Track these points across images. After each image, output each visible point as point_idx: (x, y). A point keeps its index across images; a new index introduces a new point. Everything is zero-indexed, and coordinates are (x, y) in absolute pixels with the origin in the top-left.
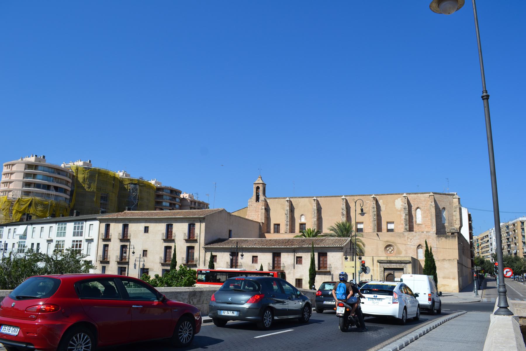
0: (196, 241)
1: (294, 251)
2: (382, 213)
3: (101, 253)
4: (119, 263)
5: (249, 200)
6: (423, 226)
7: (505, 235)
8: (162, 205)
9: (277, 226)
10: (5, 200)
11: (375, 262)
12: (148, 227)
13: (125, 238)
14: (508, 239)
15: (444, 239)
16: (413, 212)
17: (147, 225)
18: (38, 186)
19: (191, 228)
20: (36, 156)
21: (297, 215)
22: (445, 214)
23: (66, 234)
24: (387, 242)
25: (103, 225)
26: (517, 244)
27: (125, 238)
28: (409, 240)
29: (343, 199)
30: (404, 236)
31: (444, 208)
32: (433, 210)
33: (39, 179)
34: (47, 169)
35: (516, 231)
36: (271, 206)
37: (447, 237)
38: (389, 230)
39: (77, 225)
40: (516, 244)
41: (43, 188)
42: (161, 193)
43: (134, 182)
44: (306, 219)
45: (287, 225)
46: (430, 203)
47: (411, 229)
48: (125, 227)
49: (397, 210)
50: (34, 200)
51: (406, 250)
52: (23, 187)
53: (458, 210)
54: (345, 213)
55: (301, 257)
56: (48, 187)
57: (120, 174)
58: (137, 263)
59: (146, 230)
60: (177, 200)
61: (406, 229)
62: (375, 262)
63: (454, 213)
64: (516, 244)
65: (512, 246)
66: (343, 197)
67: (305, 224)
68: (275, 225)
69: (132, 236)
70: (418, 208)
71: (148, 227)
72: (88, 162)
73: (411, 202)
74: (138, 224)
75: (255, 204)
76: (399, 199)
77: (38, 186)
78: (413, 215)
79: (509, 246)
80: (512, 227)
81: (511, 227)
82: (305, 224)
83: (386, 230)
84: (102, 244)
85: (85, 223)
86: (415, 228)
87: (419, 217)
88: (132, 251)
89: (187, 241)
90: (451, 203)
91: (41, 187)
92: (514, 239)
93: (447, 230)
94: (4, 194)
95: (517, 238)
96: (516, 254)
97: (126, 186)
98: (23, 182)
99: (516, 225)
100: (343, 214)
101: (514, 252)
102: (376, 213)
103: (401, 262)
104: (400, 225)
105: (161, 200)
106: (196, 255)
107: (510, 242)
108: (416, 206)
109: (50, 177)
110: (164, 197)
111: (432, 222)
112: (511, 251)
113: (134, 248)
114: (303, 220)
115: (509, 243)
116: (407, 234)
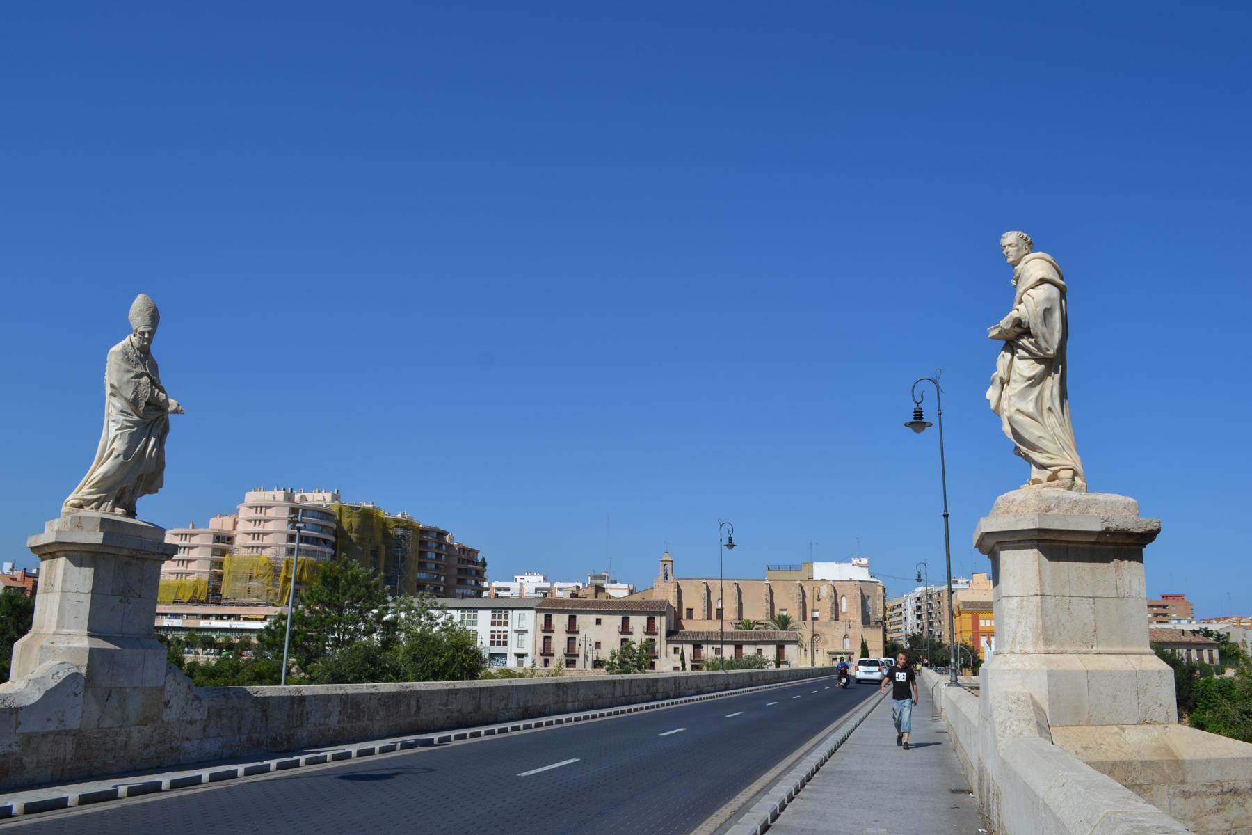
0: (656, 634)
1: (755, 643)
3: (540, 644)
4: (566, 655)
5: (655, 580)
6: (848, 615)
8: (426, 557)
9: (690, 611)
10: (265, 562)
11: (825, 653)
12: (600, 619)
13: (572, 628)
15: (869, 629)
16: (839, 600)
17: (599, 616)
18: (305, 539)
19: (651, 621)
20: (284, 490)
22: (869, 602)
23: (478, 623)
25: (542, 616)
26: (942, 623)
27: (572, 628)
28: (836, 629)
29: (767, 584)
31: (868, 597)
32: (859, 600)
33: (309, 530)
34: (316, 514)
37: (872, 627)
38: (814, 619)
39: (497, 614)
40: (940, 622)
41: (312, 544)
42: (425, 537)
43: (401, 525)
45: (704, 611)
46: (855, 591)
47: (837, 619)
48: (572, 620)
50: (306, 562)
51: (832, 640)
52: (287, 542)
53: (882, 598)
54: (769, 599)
55: (761, 649)
56: (315, 541)
57: (399, 516)
58: (590, 656)
59: (598, 622)
60: (444, 547)
61: (832, 618)
62: (825, 653)
63: (878, 602)
64: (940, 622)
65: (936, 624)
66: (767, 582)
68: (687, 609)
69: (581, 627)
70: (843, 596)
71: (600, 619)
72: (336, 493)
73: (836, 588)
74: (588, 616)
75: (662, 585)
76: (825, 586)
77: (305, 539)
78: (839, 603)
79: (931, 624)
81: (935, 596)
84: (541, 636)
85: (510, 611)
86: (841, 617)
87: (844, 605)
88: (588, 643)
89: (646, 633)
90: (875, 591)
91: (310, 541)
92: (938, 614)
93: (872, 619)
94: (252, 552)
95: (942, 613)
96: (940, 636)
97: (391, 532)
98: (288, 534)
99: (941, 594)
100: (767, 601)
101: (937, 633)
102: (801, 600)
104: (824, 612)
105: (426, 550)
106: (657, 648)
107: (933, 618)
108: (842, 594)
109: (319, 525)
110: (430, 544)
111: (857, 611)
113: (591, 641)
115: (931, 620)
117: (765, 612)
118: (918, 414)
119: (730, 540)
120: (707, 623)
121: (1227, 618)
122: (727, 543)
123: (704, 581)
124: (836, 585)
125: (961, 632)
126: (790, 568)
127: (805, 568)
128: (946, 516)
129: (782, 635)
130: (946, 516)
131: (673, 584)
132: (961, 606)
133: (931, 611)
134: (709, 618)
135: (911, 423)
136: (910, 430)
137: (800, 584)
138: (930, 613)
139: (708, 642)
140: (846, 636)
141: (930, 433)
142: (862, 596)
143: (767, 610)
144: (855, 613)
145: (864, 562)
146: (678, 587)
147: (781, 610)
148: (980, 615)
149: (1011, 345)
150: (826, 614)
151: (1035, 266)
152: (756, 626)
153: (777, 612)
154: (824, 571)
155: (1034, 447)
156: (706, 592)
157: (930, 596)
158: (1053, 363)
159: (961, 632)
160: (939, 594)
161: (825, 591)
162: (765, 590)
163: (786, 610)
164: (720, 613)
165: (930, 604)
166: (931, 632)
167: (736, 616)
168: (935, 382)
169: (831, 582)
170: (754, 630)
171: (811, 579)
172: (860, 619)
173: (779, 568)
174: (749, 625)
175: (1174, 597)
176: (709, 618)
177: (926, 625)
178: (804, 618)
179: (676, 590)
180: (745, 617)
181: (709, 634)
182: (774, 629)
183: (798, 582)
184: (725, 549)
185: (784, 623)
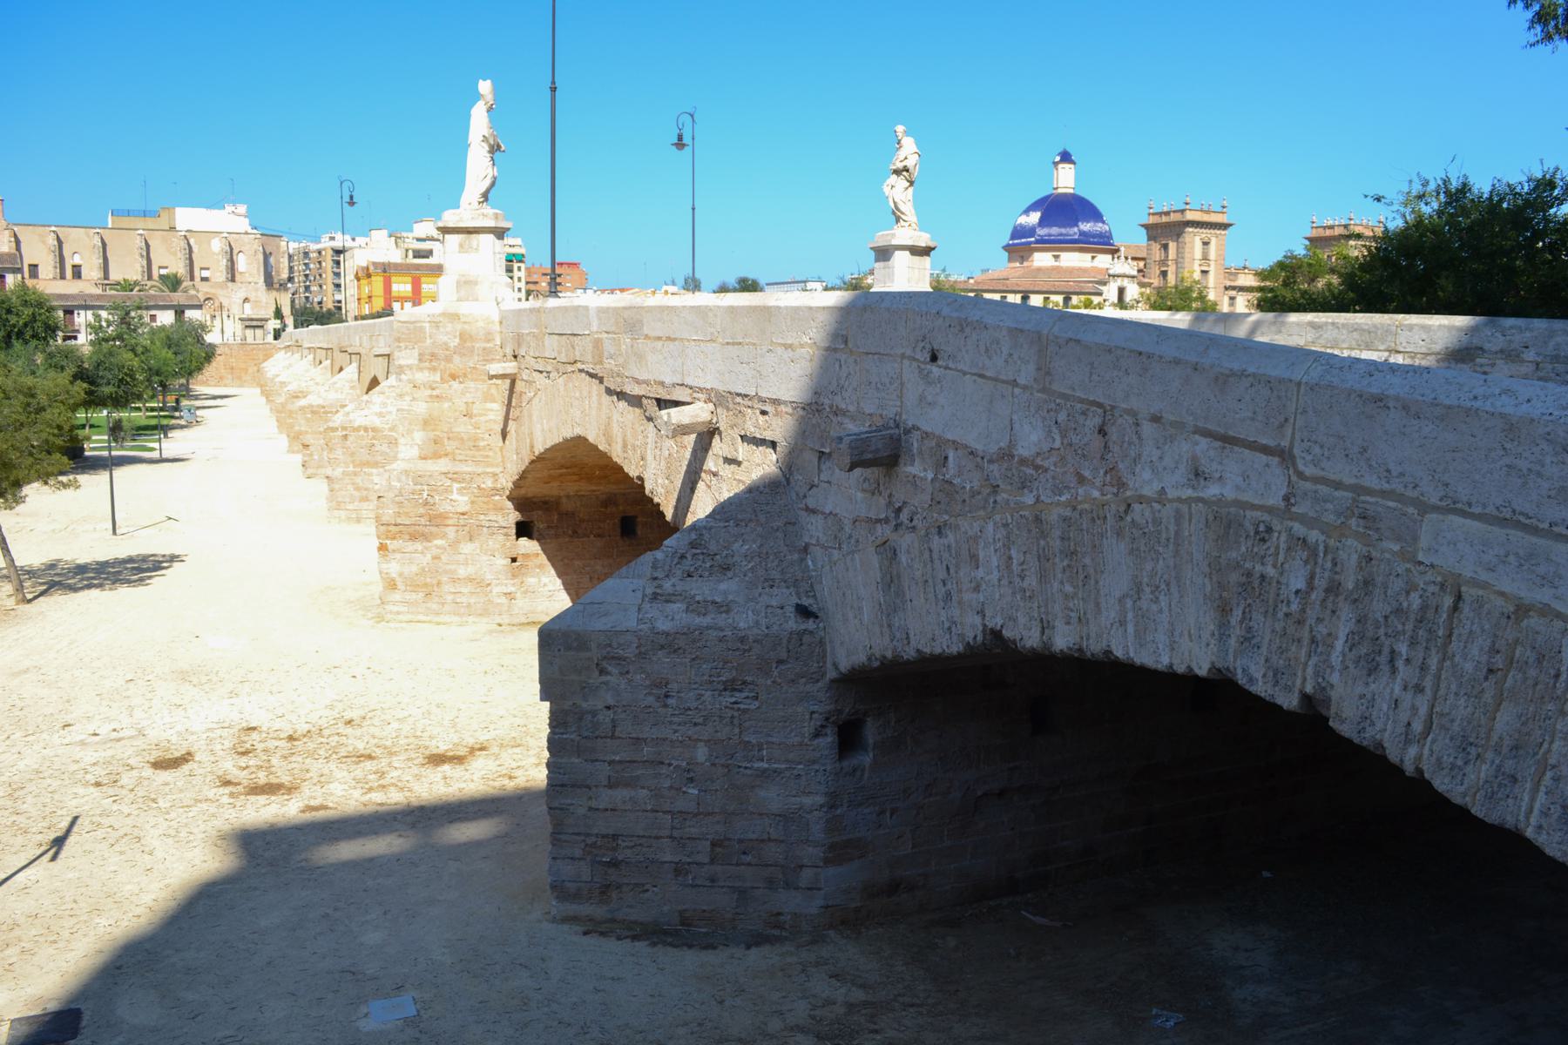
2: (194, 256)
7: (302, 267)
14: (306, 276)
16: (235, 257)
21: (66, 253)
22: (272, 260)
24: (207, 293)
26: (324, 287)
29: (141, 235)
30: (227, 287)
32: (261, 257)
35: (324, 264)
36: (21, 238)
38: (204, 279)
40: (321, 286)
44: (82, 259)
45: (56, 267)
46: (255, 246)
47: (233, 280)
49: (214, 254)
54: (145, 254)
64: (321, 286)
65: (314, 288)
66: (141, 232)
67: (80, 266)
68: (30, 265)
76: (217, 239)
79: (307, 288)
80: (315, 255)
82: (80, 266)
83: (199, 279)
86: (238, 277)
87: (242, 263)
90: (278, 247)
92: (318, 277)
93: (275, 280)
95: (324, 276)
96: (320, 303)
99: (323, 253)
100: (142, 256)
101: (316, 300)
103: (261, 320)
104: (218, 273)
112: (311, 299)
114: (77, 260)
116: (230, 284)
117: (140, 269)
118: (680, 138)
119: (351, 197)
120: (62, 282)
121: (628, 290)
122: (348, 200)
123: (53, 228)
124: (231, 238)
125: (370, 297)
126: (145, 214)
127: (164, 215)
128: (693, 209)
129: (178, 298)
130: (693, 209)
131: (7, 232)
132: (371, 268)
133: (308, 272)
134: (63, 277)
135: (676, 144)
136: (674, 147)
137: (185, 236)
138: (306, 276)
139: (86, 308)
140: (246, 300)
141: (688, 150)
142: (265, 253)
143: (143, 267)
144: (255, 272)
145: (242, 209)
146: (15, 236)
147: (160, 267)
148: (423, 279)
149: (897, 172)
150: (219, 274)
151: (909, 145)
152: (137, 288)
153: (155, 275)
154: (187, 218)
155: (903, 213)
156: (56, 243)
157: (306, 254)
158: (912, 183)
159: (370, 297)
160: (320, 253)
161: (217, 245)
162: (138, 242)
163: (166, 267)
164: (77, 272)
165: (305, 264)
166: (307, 298)
167: (101, 275)
168: (692, 116)
169: (225, 235)
170: (134, 292)
171: (173, 229)
172: (262, 279)
173: (129, 213)
174: (128, 286)
175: (569, 264)
176: (63, 277)
177: (302, 290)
178: (192, 279)
179: (13, 239)
180: (115, 276)
181: (81, 296)
182: (163, 291)
183: (183, 233)
184: (346, 205)
185: (173, 283)
